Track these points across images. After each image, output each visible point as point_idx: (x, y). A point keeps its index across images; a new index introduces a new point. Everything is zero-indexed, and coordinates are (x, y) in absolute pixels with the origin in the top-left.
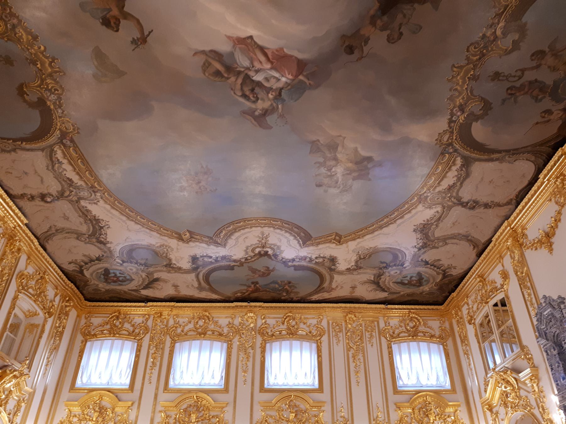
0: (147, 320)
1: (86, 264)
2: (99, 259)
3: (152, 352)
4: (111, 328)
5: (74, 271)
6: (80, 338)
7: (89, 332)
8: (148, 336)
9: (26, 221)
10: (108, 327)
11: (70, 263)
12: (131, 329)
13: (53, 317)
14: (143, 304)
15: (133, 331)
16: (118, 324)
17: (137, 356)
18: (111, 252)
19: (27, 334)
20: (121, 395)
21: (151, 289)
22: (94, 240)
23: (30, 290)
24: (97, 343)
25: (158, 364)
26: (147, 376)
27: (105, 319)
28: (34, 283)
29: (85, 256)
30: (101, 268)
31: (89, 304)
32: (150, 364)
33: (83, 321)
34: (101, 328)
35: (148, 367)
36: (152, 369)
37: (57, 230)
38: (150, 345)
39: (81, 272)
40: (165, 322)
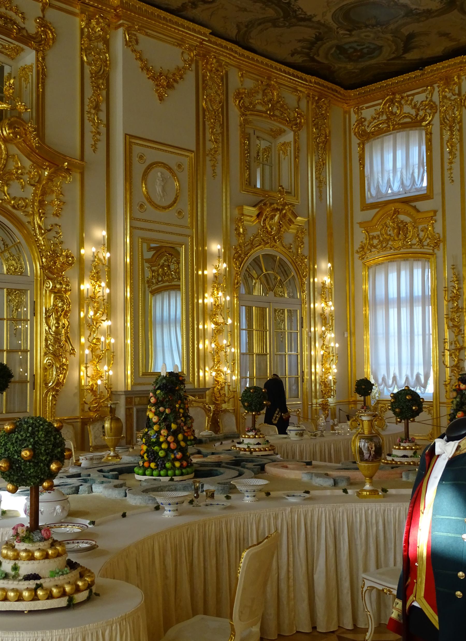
0: (432, 93)
1: (310, 49)
2: (319, 38)
3: (446, 137)
4: (388, 119)
5: (303, 61)
6: (355, 141)
7: (364, 131)
8: (437, 115)
9: (208, 31)
10: (385, 117)
11: (292, 55)
12: (413, 112)
13: (305, 127)
14: (418, 73)
15: (417, 115)
16: (395, 110)
17: (429, 149)
18: (323, 25)
19: (282, 156)
20: (418, 204)
21: (415, 50)
22: (294, 20)
23: (259, 107)
24: (376, 143)
25: (458, 153)
26: (447, 173)
27: (377, 107)
28: (260, 96)
29: (300, 41)
30: (331, 48)
31: (352, 93)
32: (447, 156)
33: (354, 117)
34: (375, 122)
35: (446, 161)
36: (451, 163)
37: (247, 26)
38: (441, 130)
39: (313, 60)
40: (457, 89)
